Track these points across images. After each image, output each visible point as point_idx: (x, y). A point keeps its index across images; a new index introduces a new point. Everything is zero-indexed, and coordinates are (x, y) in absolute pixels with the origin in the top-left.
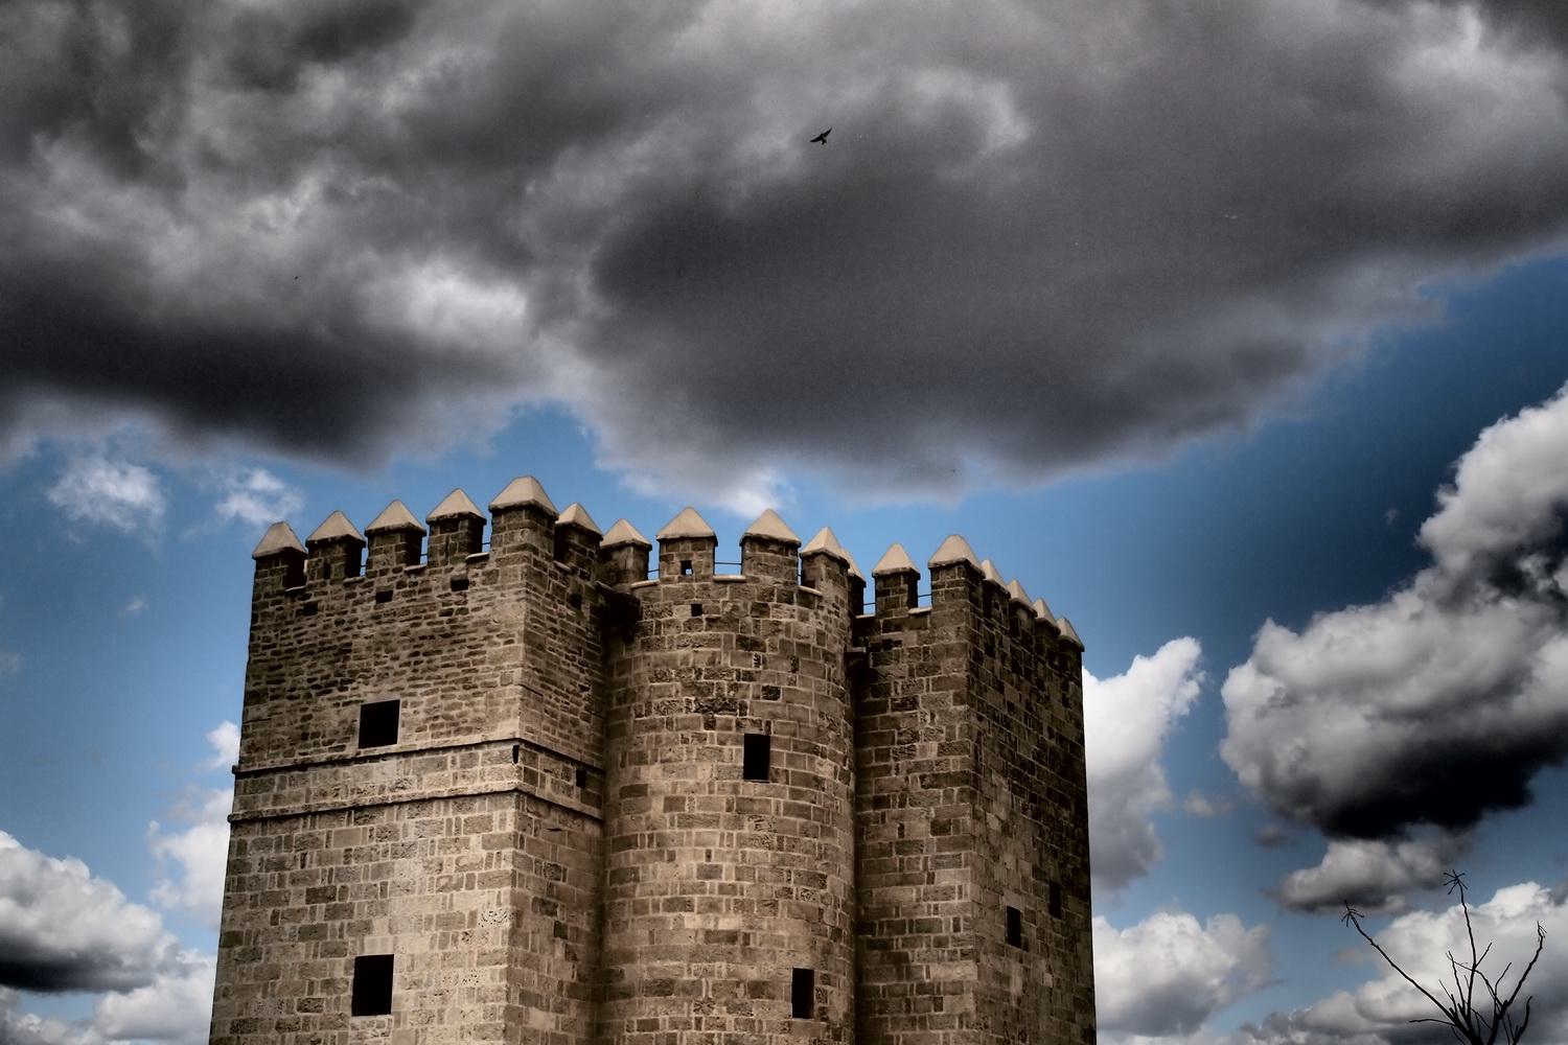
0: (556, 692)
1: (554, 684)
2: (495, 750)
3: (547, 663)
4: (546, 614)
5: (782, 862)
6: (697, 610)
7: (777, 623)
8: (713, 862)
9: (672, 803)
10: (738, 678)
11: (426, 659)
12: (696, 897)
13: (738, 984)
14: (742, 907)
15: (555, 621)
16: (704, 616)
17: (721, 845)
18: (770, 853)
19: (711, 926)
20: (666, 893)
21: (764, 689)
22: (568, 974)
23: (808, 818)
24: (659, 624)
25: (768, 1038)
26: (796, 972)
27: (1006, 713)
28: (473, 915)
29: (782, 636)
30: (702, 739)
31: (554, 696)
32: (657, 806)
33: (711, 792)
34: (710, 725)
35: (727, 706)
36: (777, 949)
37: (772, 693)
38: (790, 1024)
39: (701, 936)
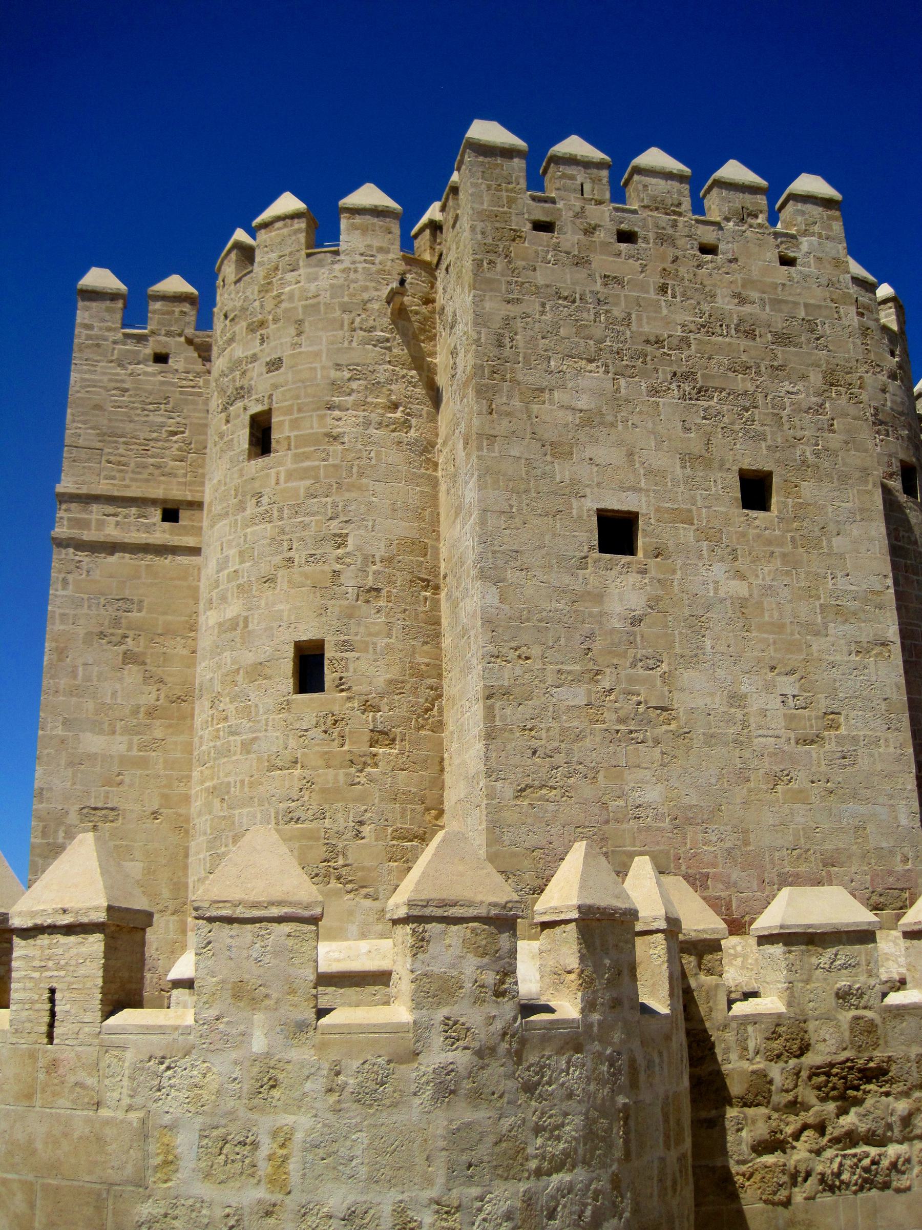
0: (126, 443)
3: (110, 420)
4: (105, 378)
5: (282, 531)
7: (279, 296)
15: (122, 381)
17: (230, 534)
18: (269, 526)
21: (267, 364)
25: (263, 722)
26: (300, 647)
27: (598, 287)
29: (284, 305)
36: (275, 625)
38: (288, 702)
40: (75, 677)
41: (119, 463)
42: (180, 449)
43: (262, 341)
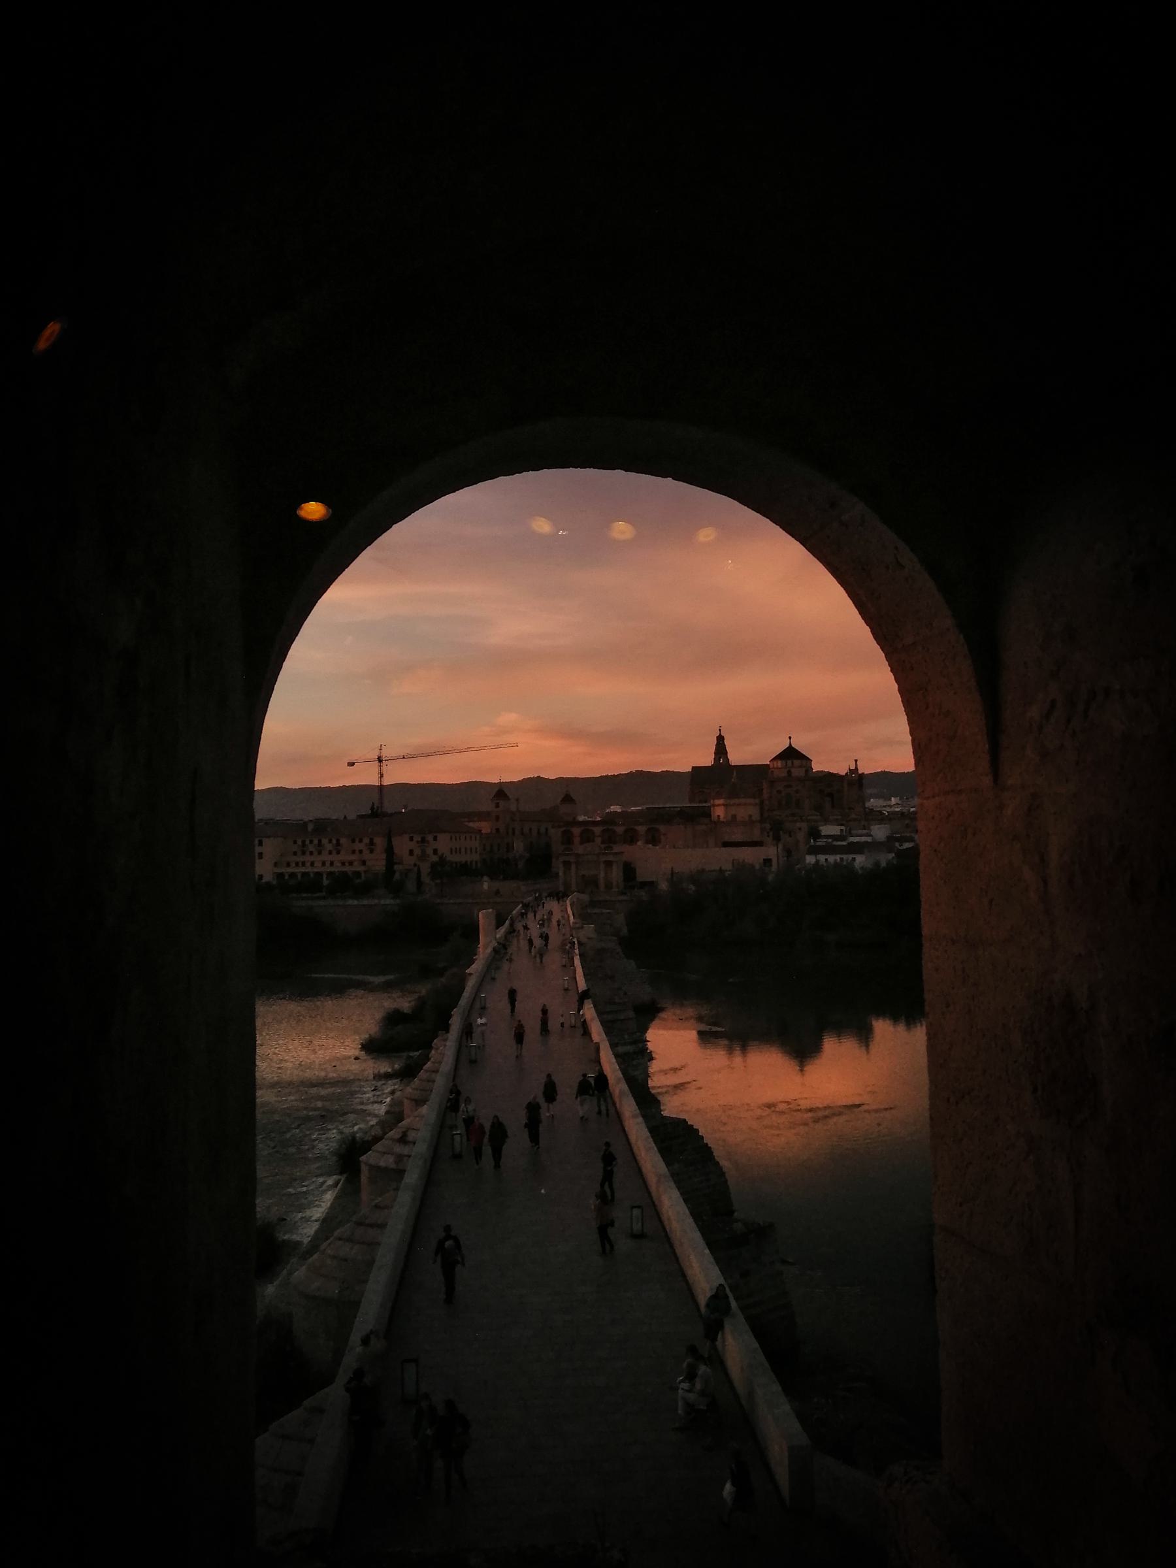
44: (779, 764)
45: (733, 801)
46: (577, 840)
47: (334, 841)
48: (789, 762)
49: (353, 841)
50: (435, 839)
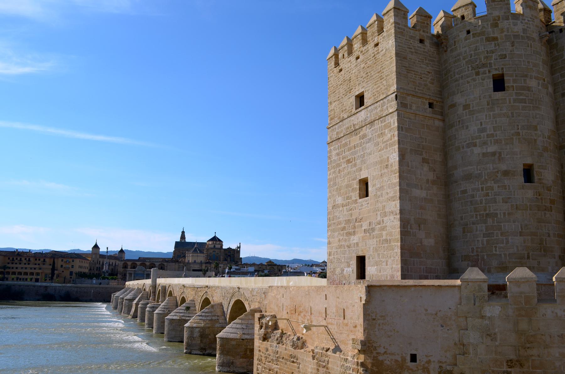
1: (414, 71)
2: (390, 98)
4: (406, 46)
6: (468, 32)
8: (483, 126)
9: (466, 107)
10: (487, 53)
11: (369, 74)
12: (478, 141)
13: (498, 172)
14: (497, 142)
15: (411, 49)
16: (471, 33)
17: (486, 119)
19: (484, 151)
20: (466, 141)
21: (499, 56)
22: (431, 176)
23: (525, 103)
24: (455, 42)
28: (388, 158)
29: (505, 33)
30: (474, 80)
31: (414, 76)
32: (460, 110)
33: (480, 99)
34: (477, 74)
35: (484, 65)
37: (504, 57)
39: (481, 155)
40: (408, 167)
41: (414, 82)
42: (431, 79)
43: (495, 46)
44: (211, 243)
45: (195, 255)
46: (129, 267)
47: (27, 259)
48: (215, 242)
49: (36, 260)
50: (73, 261)
